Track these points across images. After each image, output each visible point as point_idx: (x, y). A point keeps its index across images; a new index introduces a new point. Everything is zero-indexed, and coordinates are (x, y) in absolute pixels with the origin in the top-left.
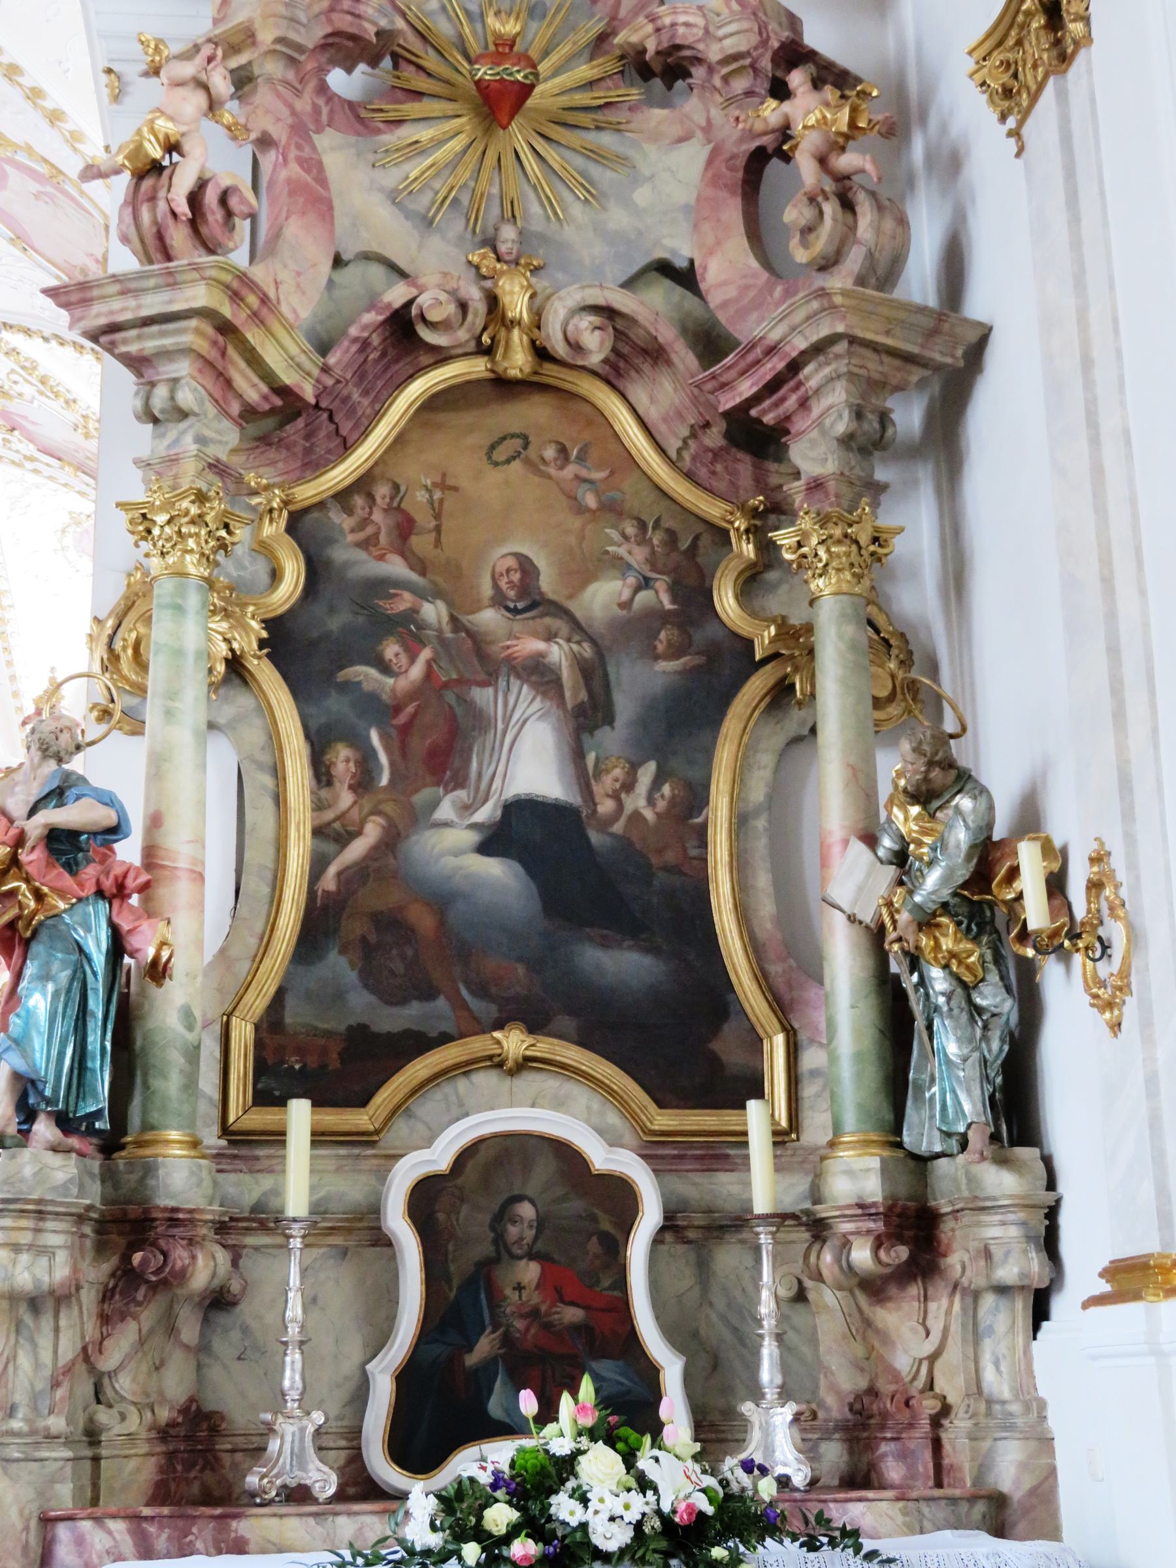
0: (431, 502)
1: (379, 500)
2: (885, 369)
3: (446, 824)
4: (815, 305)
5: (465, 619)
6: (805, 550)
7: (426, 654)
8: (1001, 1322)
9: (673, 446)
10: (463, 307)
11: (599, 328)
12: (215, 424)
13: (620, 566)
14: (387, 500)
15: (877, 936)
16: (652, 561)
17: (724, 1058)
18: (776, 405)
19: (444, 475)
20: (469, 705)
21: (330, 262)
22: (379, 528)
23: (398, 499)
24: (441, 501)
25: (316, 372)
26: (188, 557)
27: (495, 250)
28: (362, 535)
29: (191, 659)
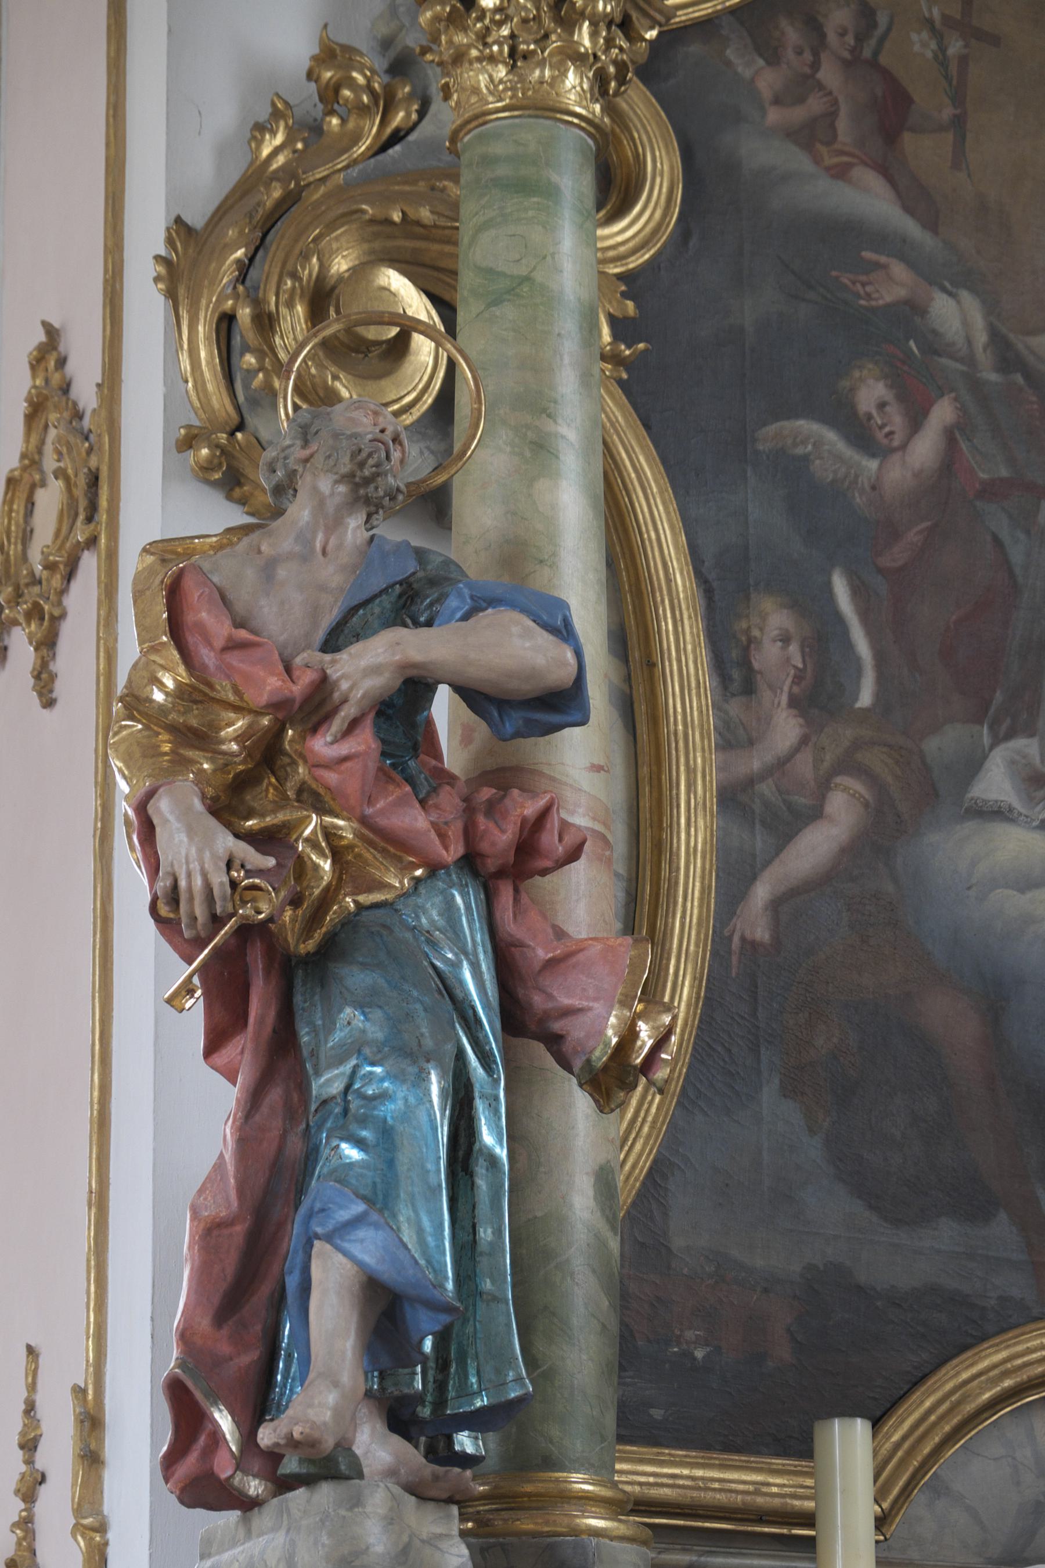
0: (941, 59)
1: (832, 38)
3: (999, 813)
14: (850, 39)
22: (835, 102)
23: (873, 42)
28: (798, 114)
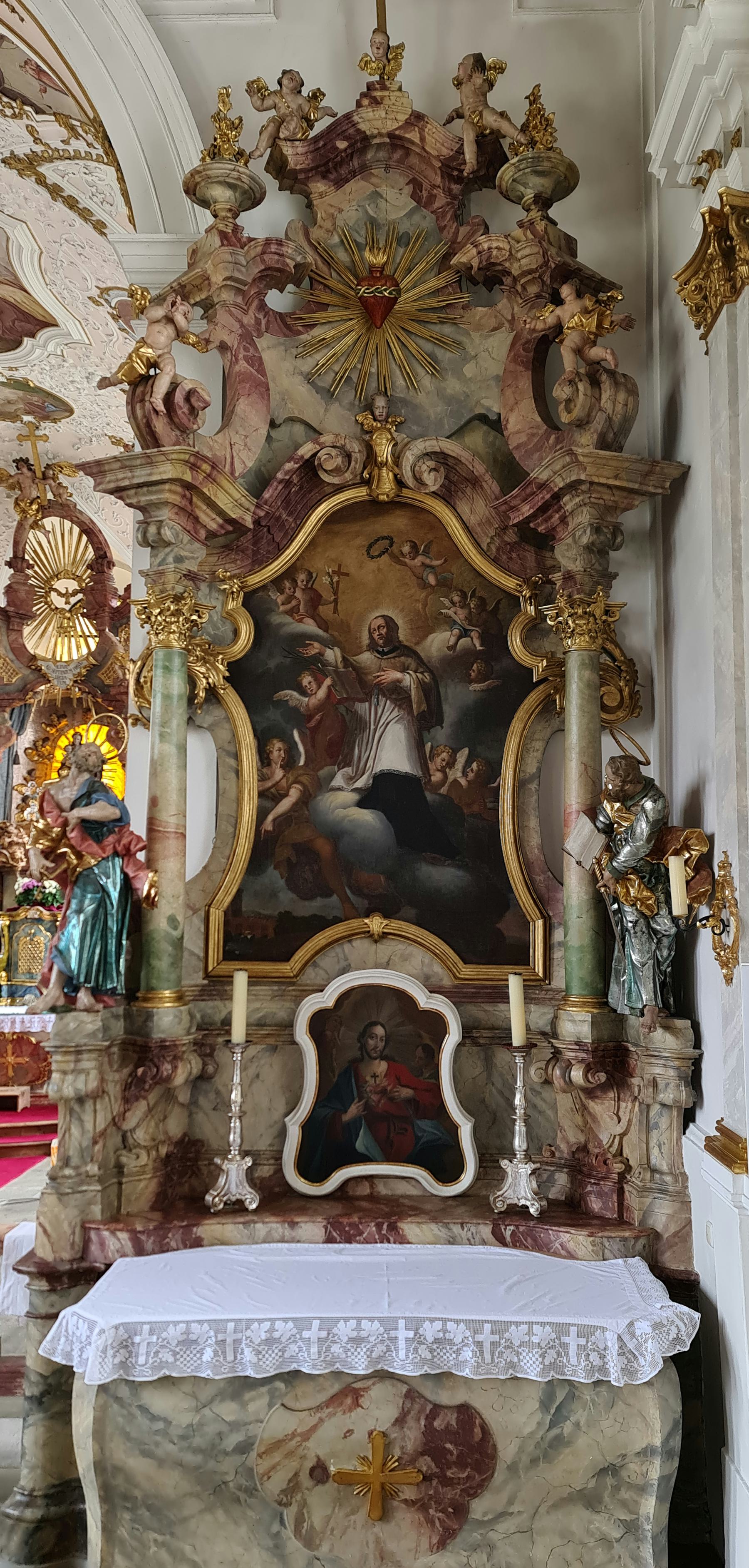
0: (331, 583)
1: (299, 583)
2: (616, 499)
3: (339, 789)
4: (568, 459)
5: (351, 659)
6: (561, 619)
7: (328, 682)
8: (664, 1122)
9: (485, 542)
10: (348, 456)
11: (434, 469)
12: (189, 546)
13: (451, 623)
15: (594, 879)
16: (469, 619)
17: (506, 933)
18: (546, 521)
19: (340, 566)
20: (355, 714)
21: (267, 426)
24: (338, 582)
25: (252, 508)
26: (172, 636)
27: (373, 414)
28: (289, 606)
29: (175, 700)
